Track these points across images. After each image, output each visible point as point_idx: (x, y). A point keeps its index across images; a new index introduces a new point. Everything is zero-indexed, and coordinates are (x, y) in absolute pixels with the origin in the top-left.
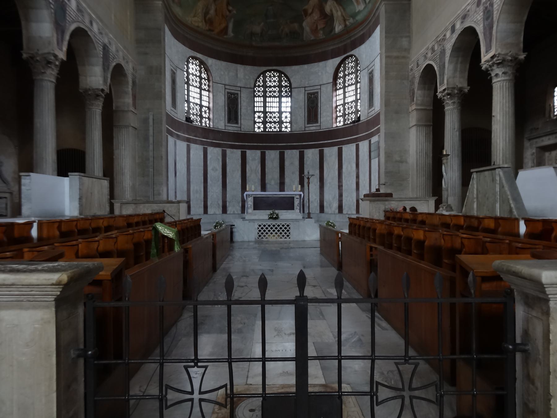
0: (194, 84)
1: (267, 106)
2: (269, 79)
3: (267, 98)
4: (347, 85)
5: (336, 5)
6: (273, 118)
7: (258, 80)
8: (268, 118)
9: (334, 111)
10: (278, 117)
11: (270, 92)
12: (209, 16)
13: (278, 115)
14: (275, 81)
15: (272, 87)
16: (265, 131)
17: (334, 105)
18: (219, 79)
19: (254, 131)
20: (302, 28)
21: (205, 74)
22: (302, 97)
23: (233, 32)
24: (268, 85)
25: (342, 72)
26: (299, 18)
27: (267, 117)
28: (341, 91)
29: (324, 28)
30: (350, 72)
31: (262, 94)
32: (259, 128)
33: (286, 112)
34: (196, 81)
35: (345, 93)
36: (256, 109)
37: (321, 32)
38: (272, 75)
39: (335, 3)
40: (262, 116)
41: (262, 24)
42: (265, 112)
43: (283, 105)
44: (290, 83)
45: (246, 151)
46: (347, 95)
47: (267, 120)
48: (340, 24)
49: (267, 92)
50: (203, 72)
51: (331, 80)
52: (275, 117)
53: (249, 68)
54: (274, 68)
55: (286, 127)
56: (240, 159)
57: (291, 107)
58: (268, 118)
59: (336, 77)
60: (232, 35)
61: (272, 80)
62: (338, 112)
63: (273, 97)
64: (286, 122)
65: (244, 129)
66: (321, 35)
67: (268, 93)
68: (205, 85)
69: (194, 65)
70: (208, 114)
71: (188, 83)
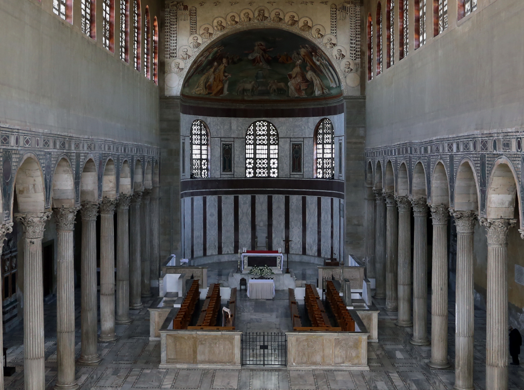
0: (196, 142)
1: (257, 153)
2: (259, 128)
3: (257, 146)
4: (325, 142)
5: (315, 75)
6: (262, 164)
7: (249, 129)
8: (258, 164)
9: (315, 163)
10: (267, 163)
11: (260, 140)
12: (209, 83)
13: (267, 161)
14: (264, 130)
15: (262, 135)
16: (255, 176)
17: (315, 157)
18: (216, 134)
19: (246, 176)
20: (288, 87)
21: (204, 130)
22: (287, 147)
23: (228, 91)
24: (258, 134)
25: (321, 130)
26: (285, 80)
27: (257, 163)
28: (320, 146)
29: (306, 89)
30: (328, 132)
31: (253, 142)
32: (250, 173)
33: (274, 159)
34: (198, 139)
35: (323, 149)
36: (247, 156)
37: (304, 92)
38: (262, 125)
39: (314, 74)
40: (253, 162)
41: (253, 82)
42: (255, 159)
43: (271, 152)
44: (277, 132)
45: (238, 196)
46: (325, 151)
47: (257, 166)
48: (319, 90)
49: (257, 140)
50: (203, 129)
51: (312, 136)
52: (264, 163)
53: (241, 119)
54: (264, 119)
55: (274, 173)
56: (233, 204)
57: (278, 154)
58: (258, 164)
59: (316, 133)
60: (227, 93)
61: (262, 128)
62: (318, 164)
63: (262, 145)
64: (274, 168)
65: (236, 175)
66: (304, 95)
67: (258, 141)
68: (204, 140)
69: (196, 126)
70: (206, 165)
71: (192, 144)
